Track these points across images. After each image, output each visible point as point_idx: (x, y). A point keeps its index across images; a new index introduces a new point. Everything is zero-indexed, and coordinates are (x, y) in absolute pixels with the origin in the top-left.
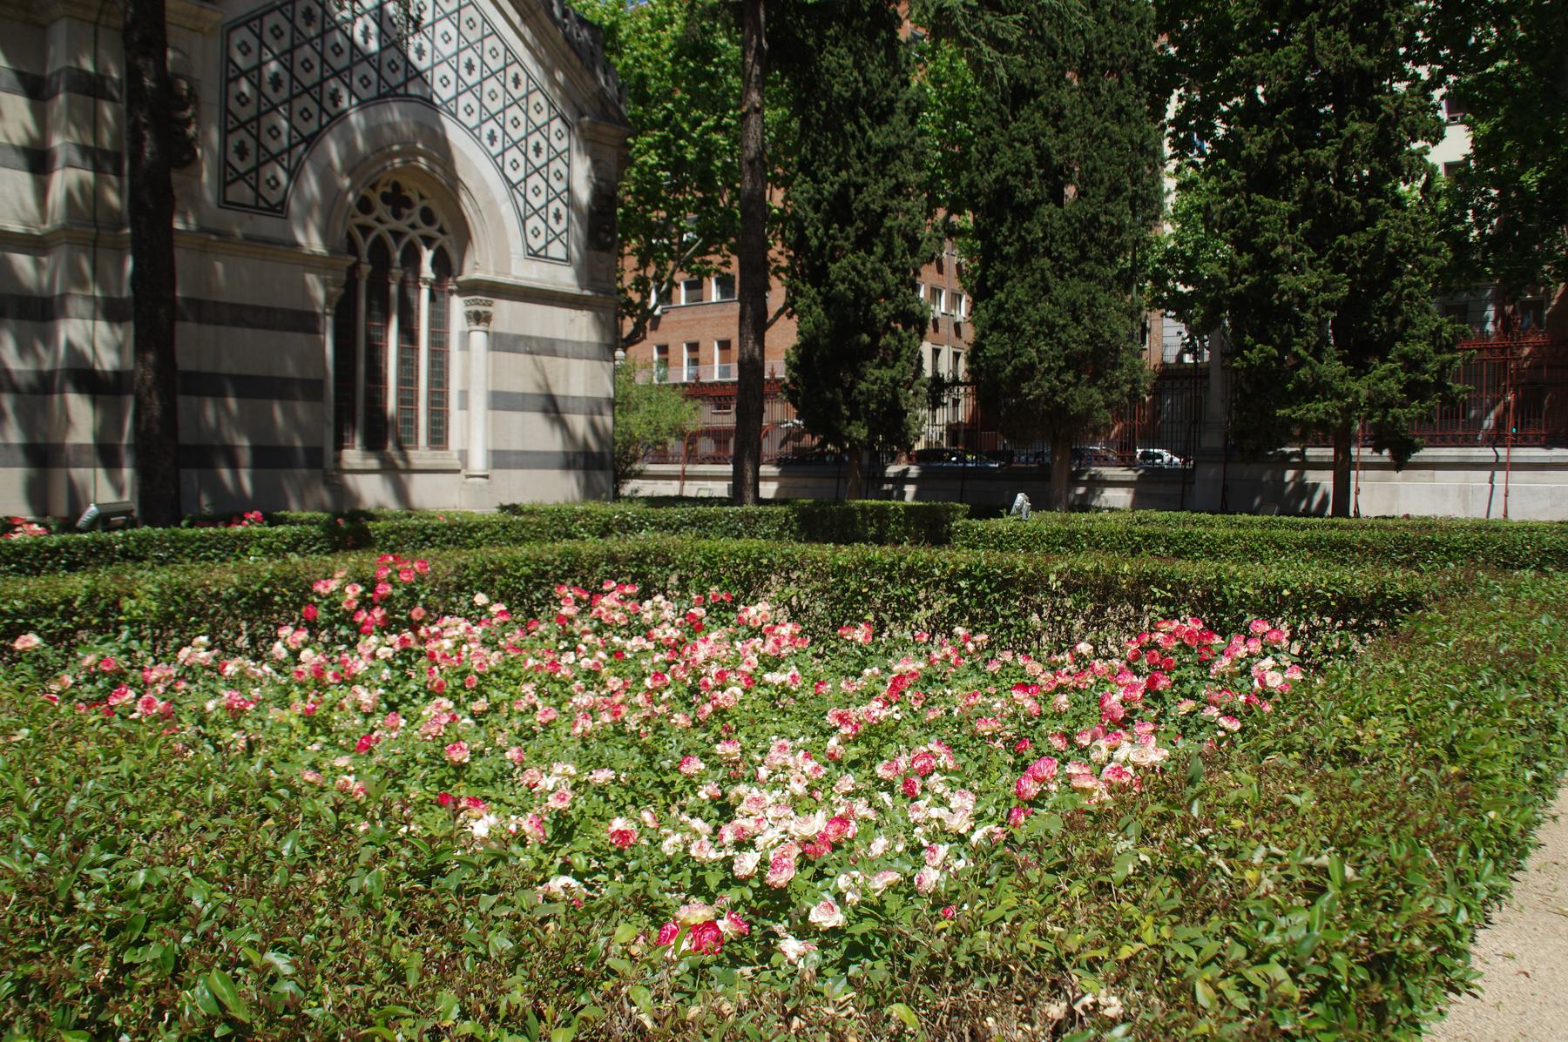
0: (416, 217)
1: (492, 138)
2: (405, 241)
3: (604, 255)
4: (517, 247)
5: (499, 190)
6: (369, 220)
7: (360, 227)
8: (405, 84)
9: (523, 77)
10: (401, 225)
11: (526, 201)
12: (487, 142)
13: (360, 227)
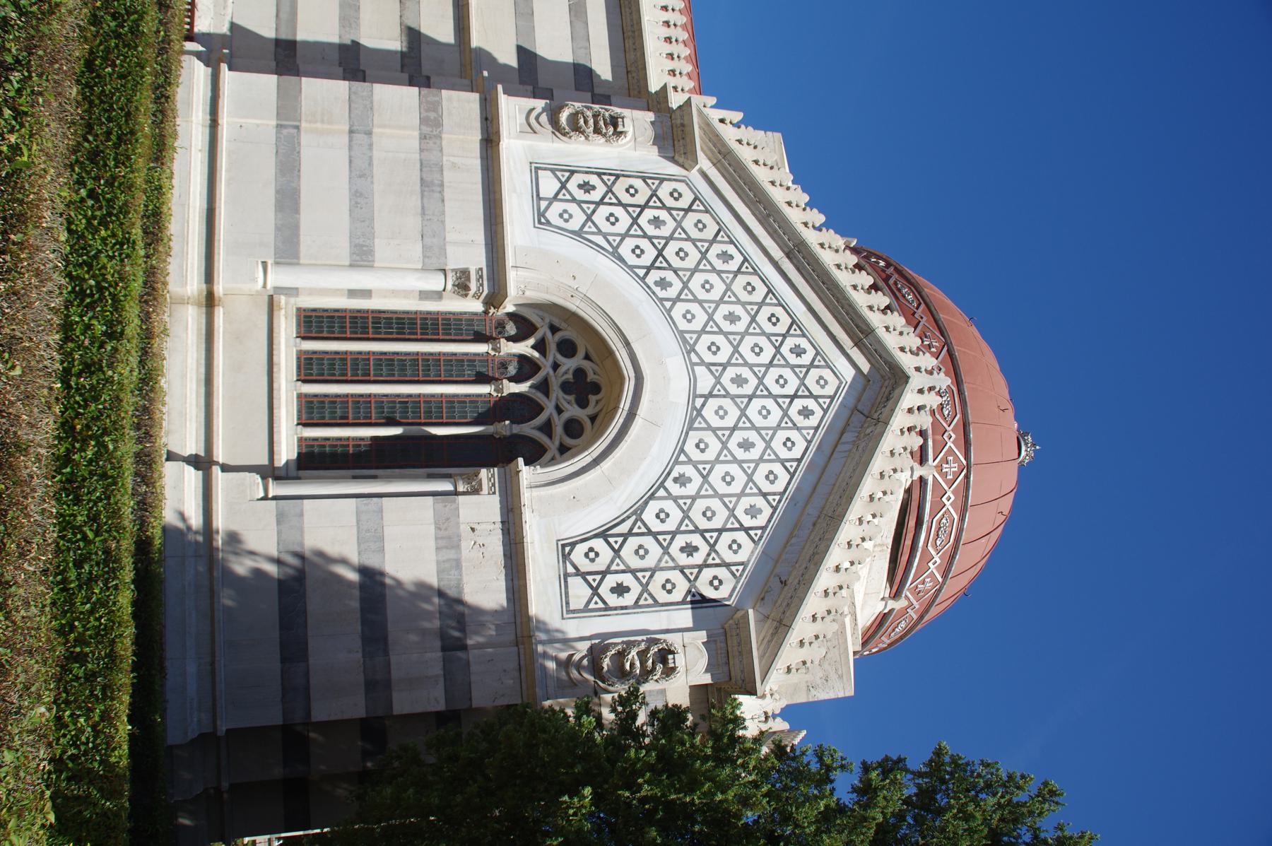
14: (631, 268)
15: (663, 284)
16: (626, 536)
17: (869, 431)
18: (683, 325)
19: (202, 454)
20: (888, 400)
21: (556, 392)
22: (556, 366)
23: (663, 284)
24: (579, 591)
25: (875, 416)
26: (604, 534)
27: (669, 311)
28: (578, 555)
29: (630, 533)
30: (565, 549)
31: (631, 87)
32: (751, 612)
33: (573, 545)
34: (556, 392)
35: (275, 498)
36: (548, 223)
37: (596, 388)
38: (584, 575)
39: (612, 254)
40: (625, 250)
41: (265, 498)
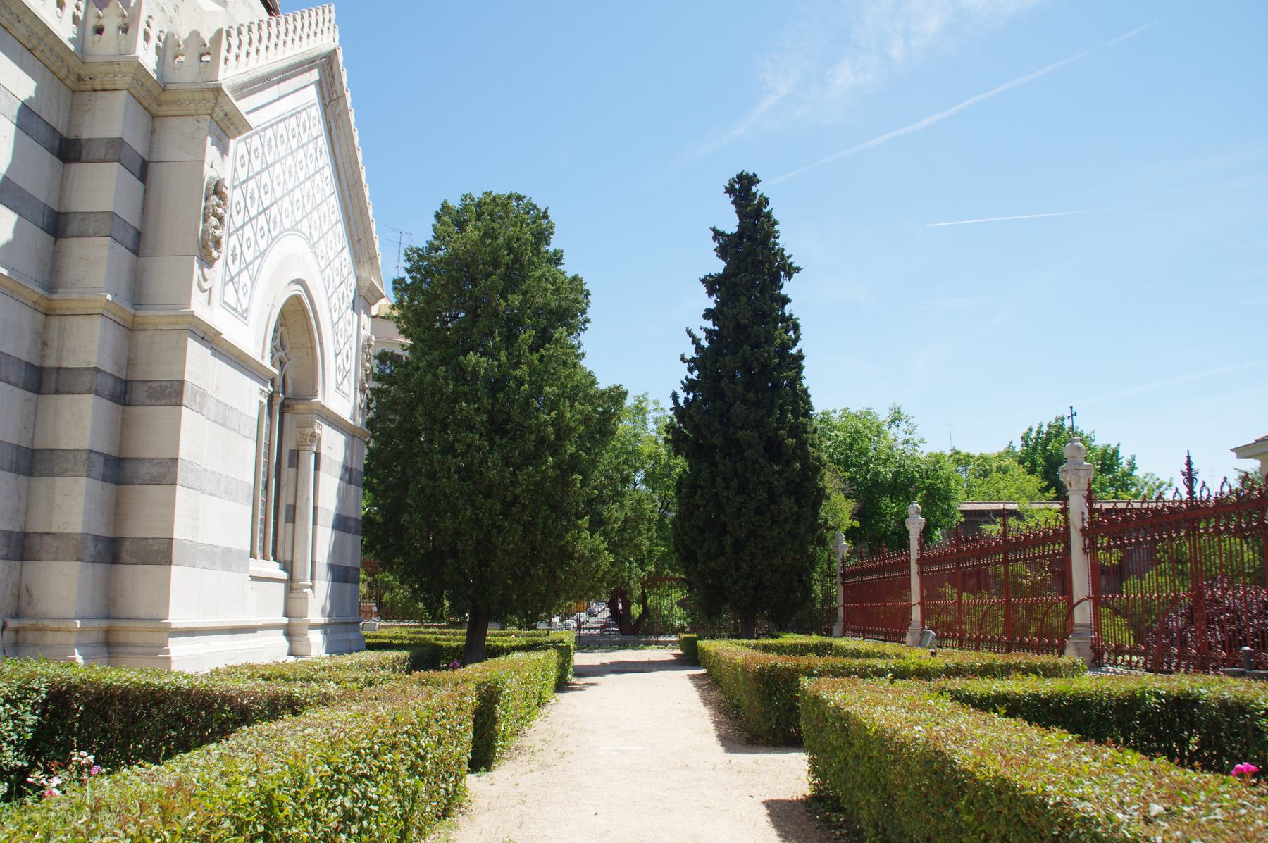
17: (338, 111)
19: (282, 631)
20: (333, 77)
25: (335, 97)
26: (337, 355)
31: (48, 63)
32: (373, 279)
35: (312, 579)
36: (247, 310)
39: (262, 258)
41: (312, 587)
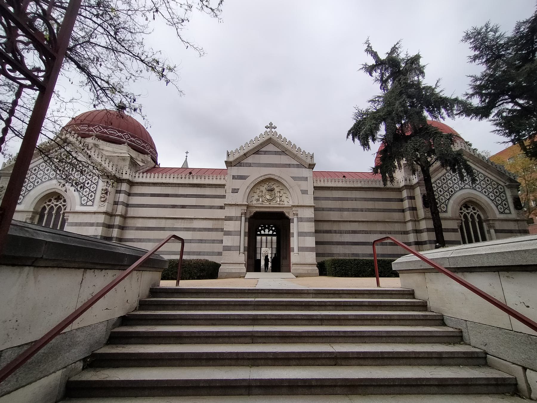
0: (471, 209)
1: (485, 192)
2: (470, 214)
3: (520, 211)
4: (497, 212)
5: (490, 202)
6: (462, 211)
7: (461, 213)
8: (464, 186)
9: (489, 179)
10: (469, 211)
11: (497, 203)
12: (484, 193)
13: (461, 213)
14: (33, 188)
15: (38, 182)
16: (83, 194)
18: (47, 180)
21: (57, 203)
22: (53, 203)
23: (38, 182)
24: (90, 203)
27: (43, 182)
28: (83, 203)
29: (82, 193)
30: (82, 205)
33: (81, 203)
34: (57, 203)
37: (59, 196)
38: (87, 202)
40: (29, 189)
